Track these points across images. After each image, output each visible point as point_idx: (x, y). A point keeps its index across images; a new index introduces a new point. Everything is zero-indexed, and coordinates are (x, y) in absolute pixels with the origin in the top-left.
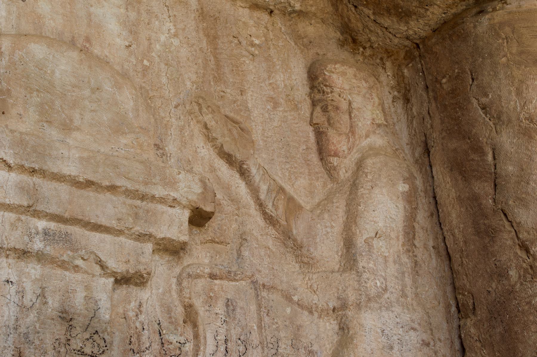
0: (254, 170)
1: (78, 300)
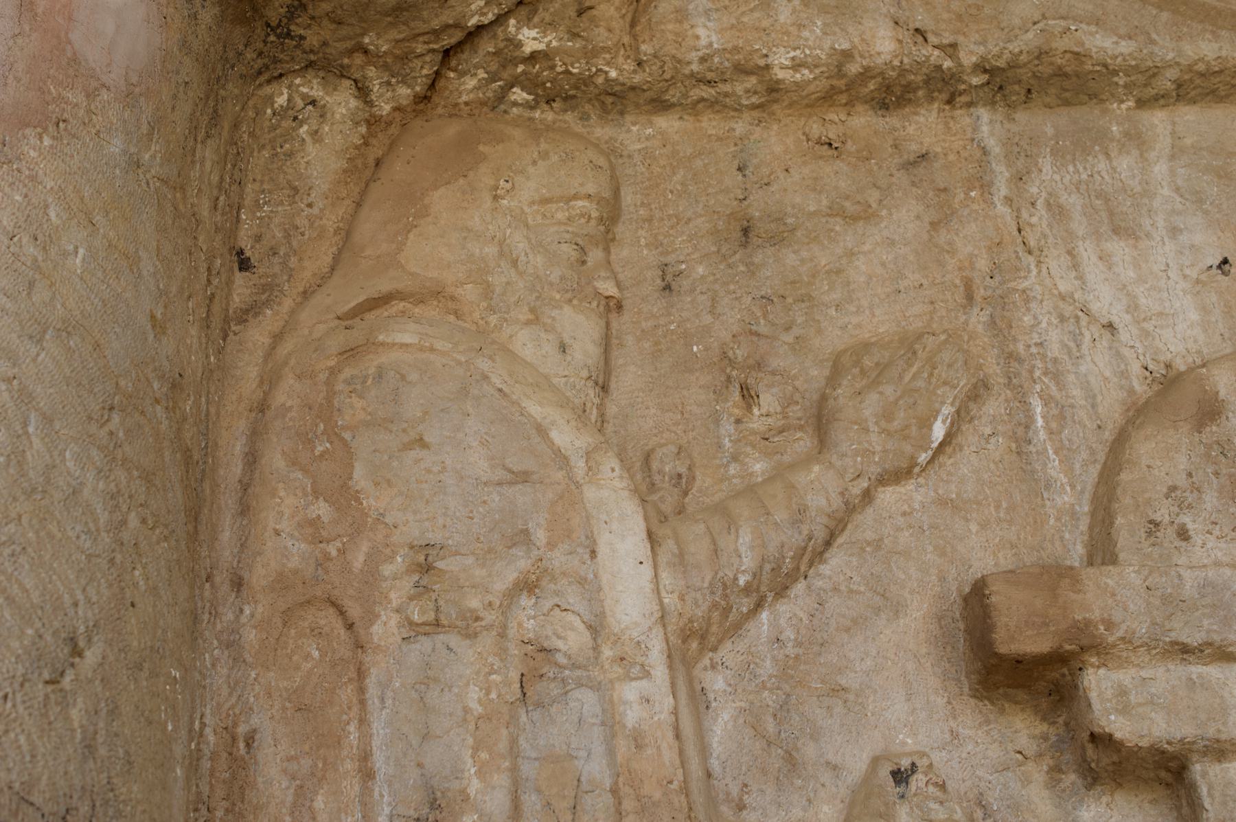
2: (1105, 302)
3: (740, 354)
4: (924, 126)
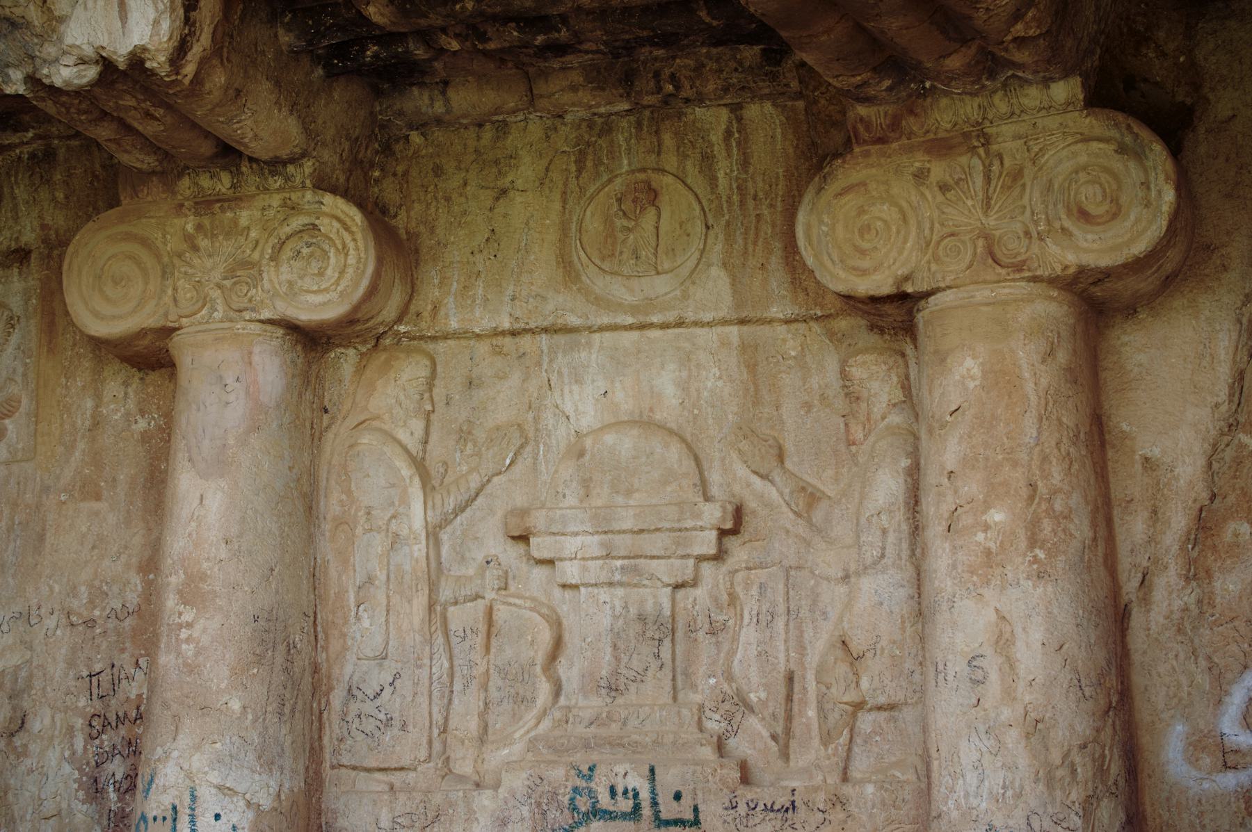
0: (777, 479)
1: (649, 607)
2: (569, 408)
4: (526, 342)
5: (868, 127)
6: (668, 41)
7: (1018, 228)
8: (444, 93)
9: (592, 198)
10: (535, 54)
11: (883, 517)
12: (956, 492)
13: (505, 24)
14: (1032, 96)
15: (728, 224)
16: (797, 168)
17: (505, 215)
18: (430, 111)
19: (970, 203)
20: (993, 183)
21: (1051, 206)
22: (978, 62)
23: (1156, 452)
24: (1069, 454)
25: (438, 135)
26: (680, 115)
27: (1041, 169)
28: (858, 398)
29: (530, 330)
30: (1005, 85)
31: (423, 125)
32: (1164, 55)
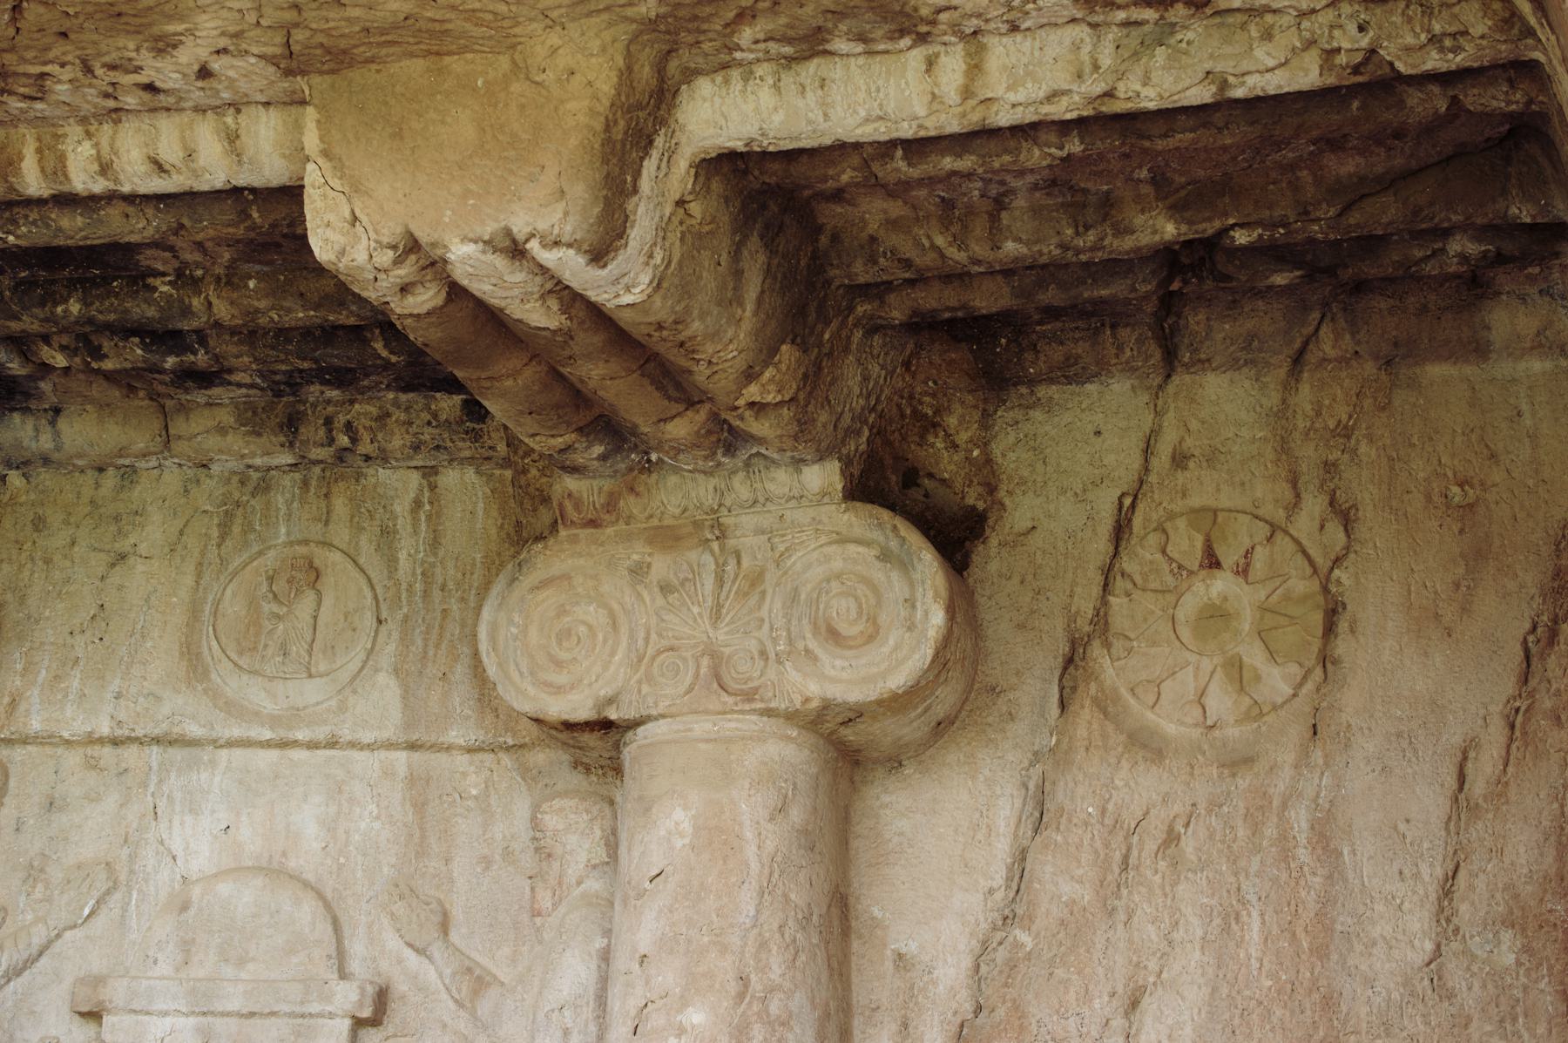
0: (437, 955)
2: (177, 846)
3: (36, 864)
4: (131, 754)
5: (578, 506)
6: (342, 378)
7: (753, 645)
8: (53, 423)
9: (235, 574)
10: (172, 381)
11: (567, 1013)
12: (647, 983)
13: (126, 339)
14: (780, 480)
15: (406, 619)
16: (499, 554)
17: (120, 588)
18: (34, 445)
19: (696, 610)
20: (726, 589)
21: (794, 622)
22: (709, 432)
23: (913, 947)
24: (794, 941)
25: (45, 477)
26: (359, 476)
27: (786, 573)
28: (549, 855)
29: (137, 739)
30: (747, 464)
31: (26, 463)
32: (955, 446)
